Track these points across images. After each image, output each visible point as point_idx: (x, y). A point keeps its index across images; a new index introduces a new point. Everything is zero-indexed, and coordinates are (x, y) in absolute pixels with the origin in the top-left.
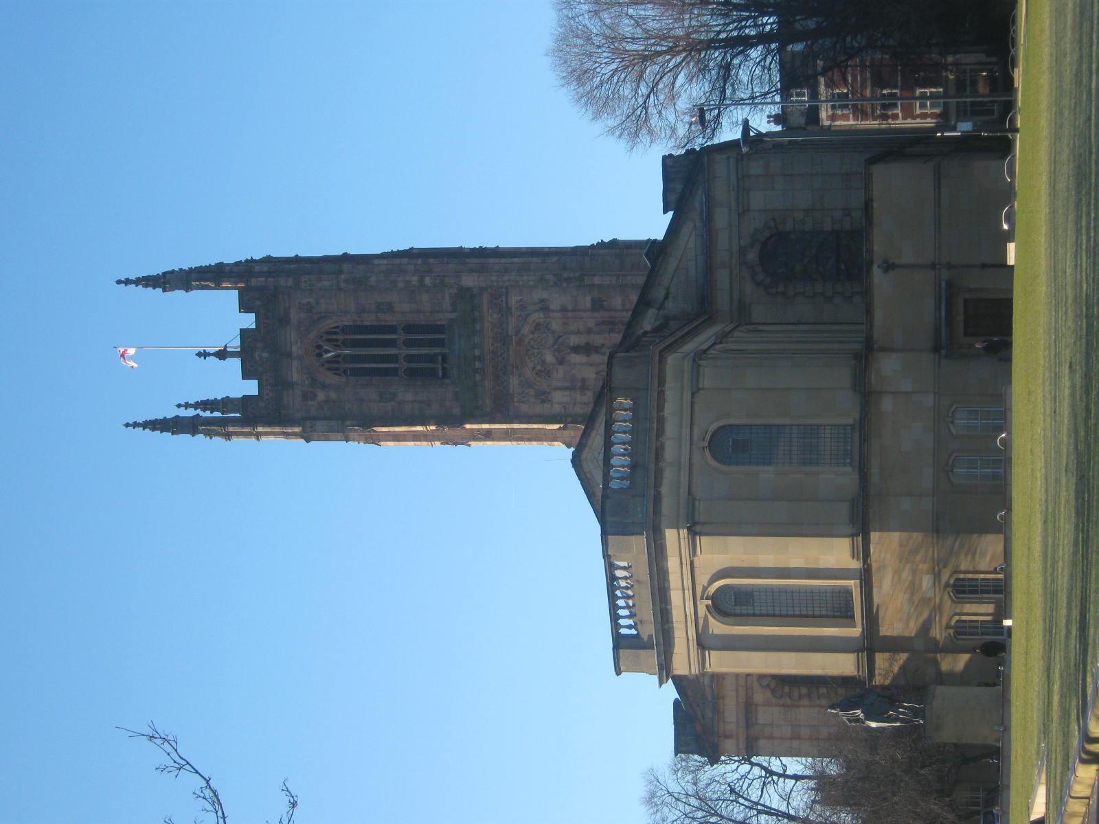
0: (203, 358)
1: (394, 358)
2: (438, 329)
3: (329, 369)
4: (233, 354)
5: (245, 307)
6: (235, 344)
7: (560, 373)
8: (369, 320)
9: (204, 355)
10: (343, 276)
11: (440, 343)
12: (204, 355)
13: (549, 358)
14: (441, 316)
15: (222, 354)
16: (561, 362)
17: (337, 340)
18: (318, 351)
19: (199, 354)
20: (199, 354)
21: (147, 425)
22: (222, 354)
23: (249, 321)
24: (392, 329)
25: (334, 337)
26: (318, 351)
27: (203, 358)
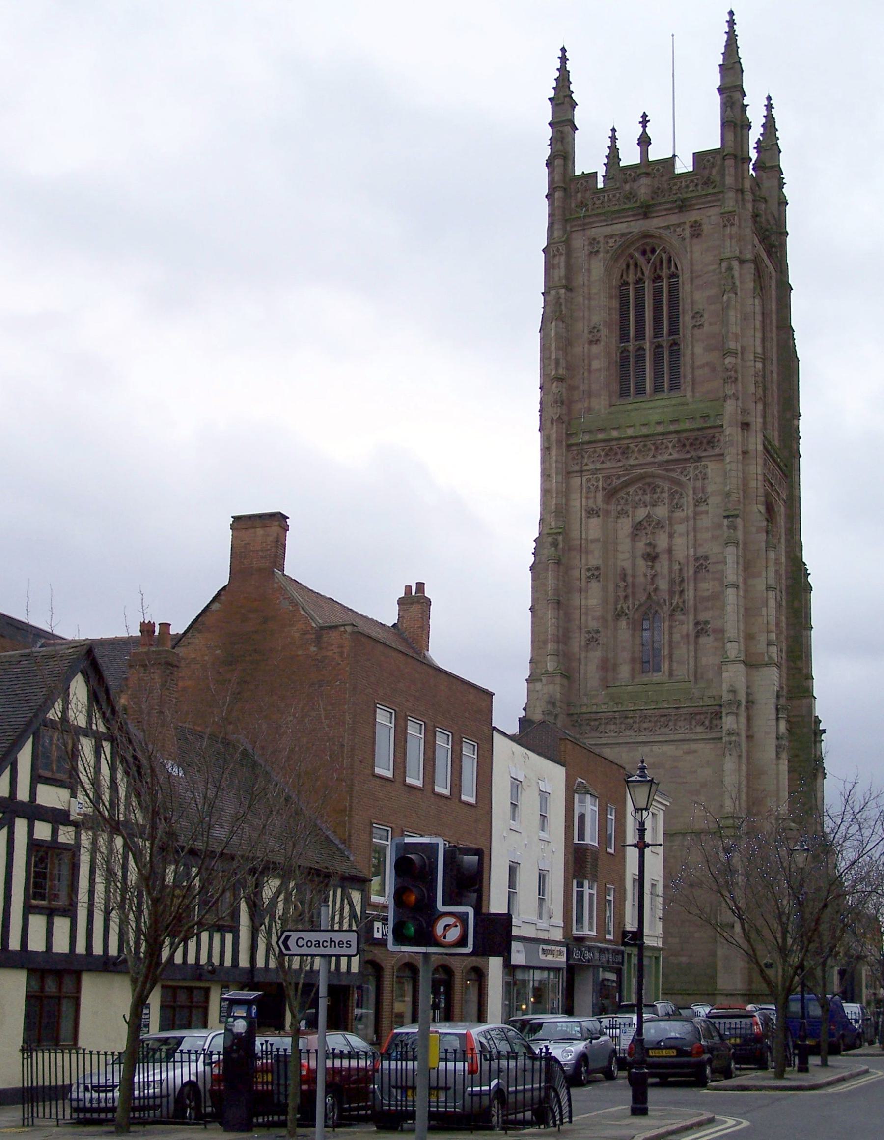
0: (641, 120)
1: (640, 334)
2: (675, 386)
3: (628, 266)
4: (644, 154)
5: (698, 157)
6: (656, 153)
7: (625, 526)
8: (685, 304)
9: (644, 121)
10: (735, 264)
11: (658, 388)
12: (644, 121)
13: (642, 513)
14: (689, 389)
15: (644, 141)
16: (638, 527)
17: (661, 268)
18: (648, 249)
19: (645, 116)
20: (645, 116)
21: (563, 80)
22: (644, 141)
23: (684, 165)
24: (674, 330)
25: (665, 265)
26: (648, 249)
27: (641, 120)
